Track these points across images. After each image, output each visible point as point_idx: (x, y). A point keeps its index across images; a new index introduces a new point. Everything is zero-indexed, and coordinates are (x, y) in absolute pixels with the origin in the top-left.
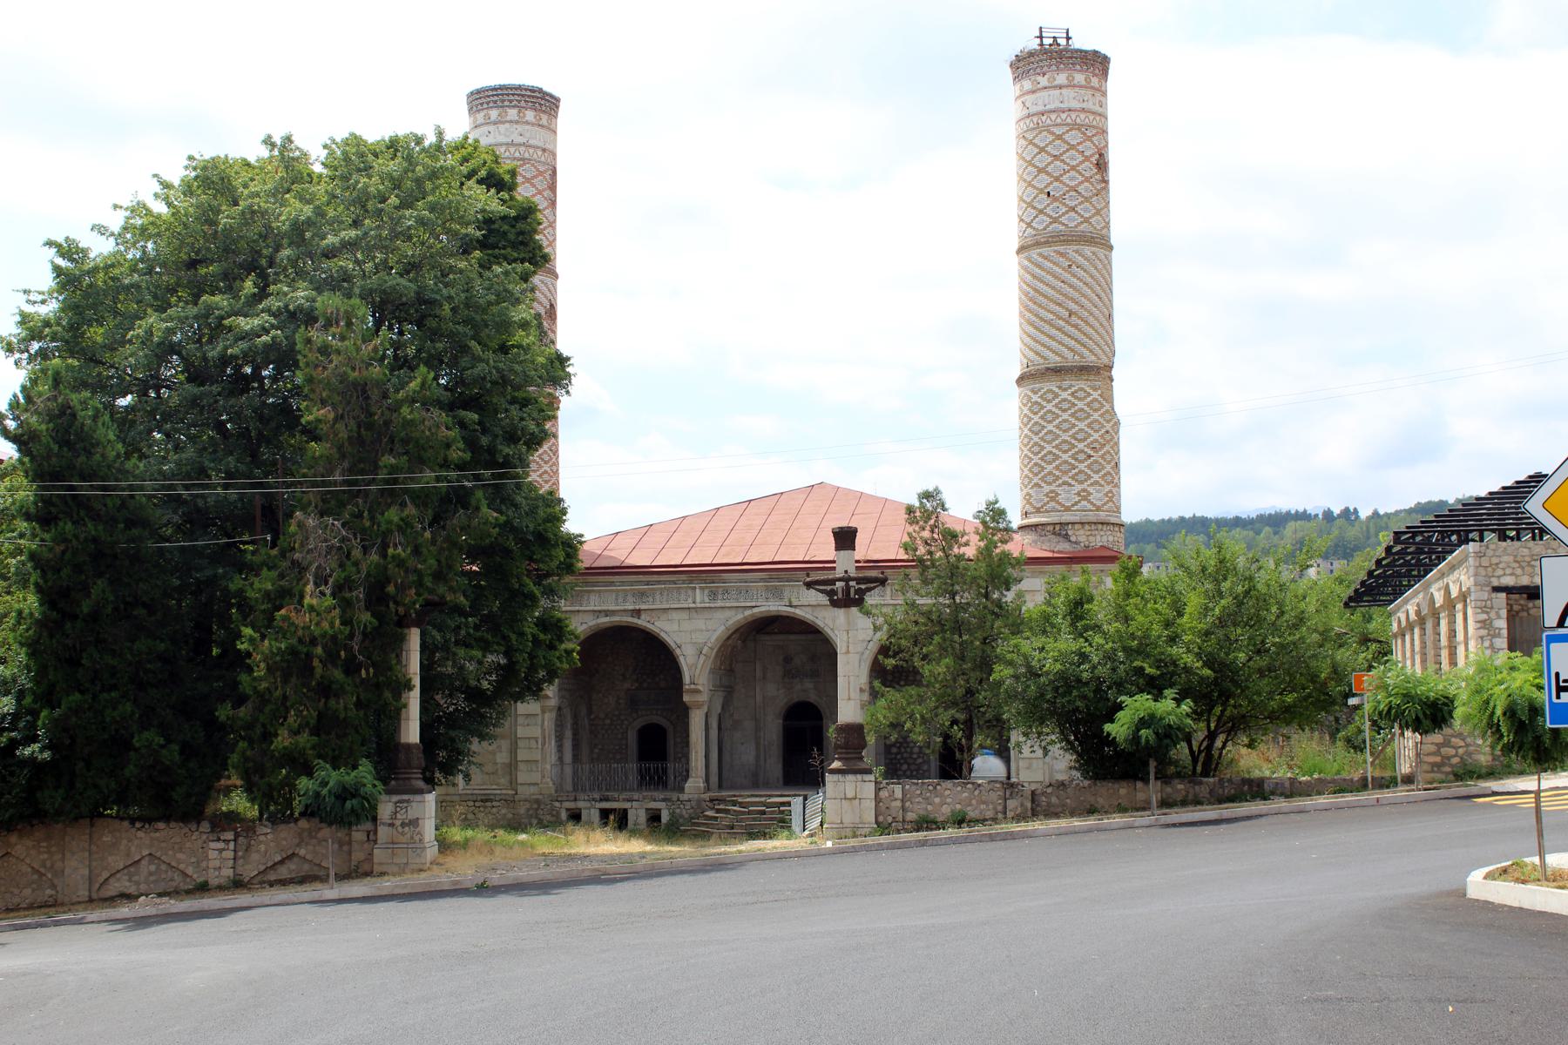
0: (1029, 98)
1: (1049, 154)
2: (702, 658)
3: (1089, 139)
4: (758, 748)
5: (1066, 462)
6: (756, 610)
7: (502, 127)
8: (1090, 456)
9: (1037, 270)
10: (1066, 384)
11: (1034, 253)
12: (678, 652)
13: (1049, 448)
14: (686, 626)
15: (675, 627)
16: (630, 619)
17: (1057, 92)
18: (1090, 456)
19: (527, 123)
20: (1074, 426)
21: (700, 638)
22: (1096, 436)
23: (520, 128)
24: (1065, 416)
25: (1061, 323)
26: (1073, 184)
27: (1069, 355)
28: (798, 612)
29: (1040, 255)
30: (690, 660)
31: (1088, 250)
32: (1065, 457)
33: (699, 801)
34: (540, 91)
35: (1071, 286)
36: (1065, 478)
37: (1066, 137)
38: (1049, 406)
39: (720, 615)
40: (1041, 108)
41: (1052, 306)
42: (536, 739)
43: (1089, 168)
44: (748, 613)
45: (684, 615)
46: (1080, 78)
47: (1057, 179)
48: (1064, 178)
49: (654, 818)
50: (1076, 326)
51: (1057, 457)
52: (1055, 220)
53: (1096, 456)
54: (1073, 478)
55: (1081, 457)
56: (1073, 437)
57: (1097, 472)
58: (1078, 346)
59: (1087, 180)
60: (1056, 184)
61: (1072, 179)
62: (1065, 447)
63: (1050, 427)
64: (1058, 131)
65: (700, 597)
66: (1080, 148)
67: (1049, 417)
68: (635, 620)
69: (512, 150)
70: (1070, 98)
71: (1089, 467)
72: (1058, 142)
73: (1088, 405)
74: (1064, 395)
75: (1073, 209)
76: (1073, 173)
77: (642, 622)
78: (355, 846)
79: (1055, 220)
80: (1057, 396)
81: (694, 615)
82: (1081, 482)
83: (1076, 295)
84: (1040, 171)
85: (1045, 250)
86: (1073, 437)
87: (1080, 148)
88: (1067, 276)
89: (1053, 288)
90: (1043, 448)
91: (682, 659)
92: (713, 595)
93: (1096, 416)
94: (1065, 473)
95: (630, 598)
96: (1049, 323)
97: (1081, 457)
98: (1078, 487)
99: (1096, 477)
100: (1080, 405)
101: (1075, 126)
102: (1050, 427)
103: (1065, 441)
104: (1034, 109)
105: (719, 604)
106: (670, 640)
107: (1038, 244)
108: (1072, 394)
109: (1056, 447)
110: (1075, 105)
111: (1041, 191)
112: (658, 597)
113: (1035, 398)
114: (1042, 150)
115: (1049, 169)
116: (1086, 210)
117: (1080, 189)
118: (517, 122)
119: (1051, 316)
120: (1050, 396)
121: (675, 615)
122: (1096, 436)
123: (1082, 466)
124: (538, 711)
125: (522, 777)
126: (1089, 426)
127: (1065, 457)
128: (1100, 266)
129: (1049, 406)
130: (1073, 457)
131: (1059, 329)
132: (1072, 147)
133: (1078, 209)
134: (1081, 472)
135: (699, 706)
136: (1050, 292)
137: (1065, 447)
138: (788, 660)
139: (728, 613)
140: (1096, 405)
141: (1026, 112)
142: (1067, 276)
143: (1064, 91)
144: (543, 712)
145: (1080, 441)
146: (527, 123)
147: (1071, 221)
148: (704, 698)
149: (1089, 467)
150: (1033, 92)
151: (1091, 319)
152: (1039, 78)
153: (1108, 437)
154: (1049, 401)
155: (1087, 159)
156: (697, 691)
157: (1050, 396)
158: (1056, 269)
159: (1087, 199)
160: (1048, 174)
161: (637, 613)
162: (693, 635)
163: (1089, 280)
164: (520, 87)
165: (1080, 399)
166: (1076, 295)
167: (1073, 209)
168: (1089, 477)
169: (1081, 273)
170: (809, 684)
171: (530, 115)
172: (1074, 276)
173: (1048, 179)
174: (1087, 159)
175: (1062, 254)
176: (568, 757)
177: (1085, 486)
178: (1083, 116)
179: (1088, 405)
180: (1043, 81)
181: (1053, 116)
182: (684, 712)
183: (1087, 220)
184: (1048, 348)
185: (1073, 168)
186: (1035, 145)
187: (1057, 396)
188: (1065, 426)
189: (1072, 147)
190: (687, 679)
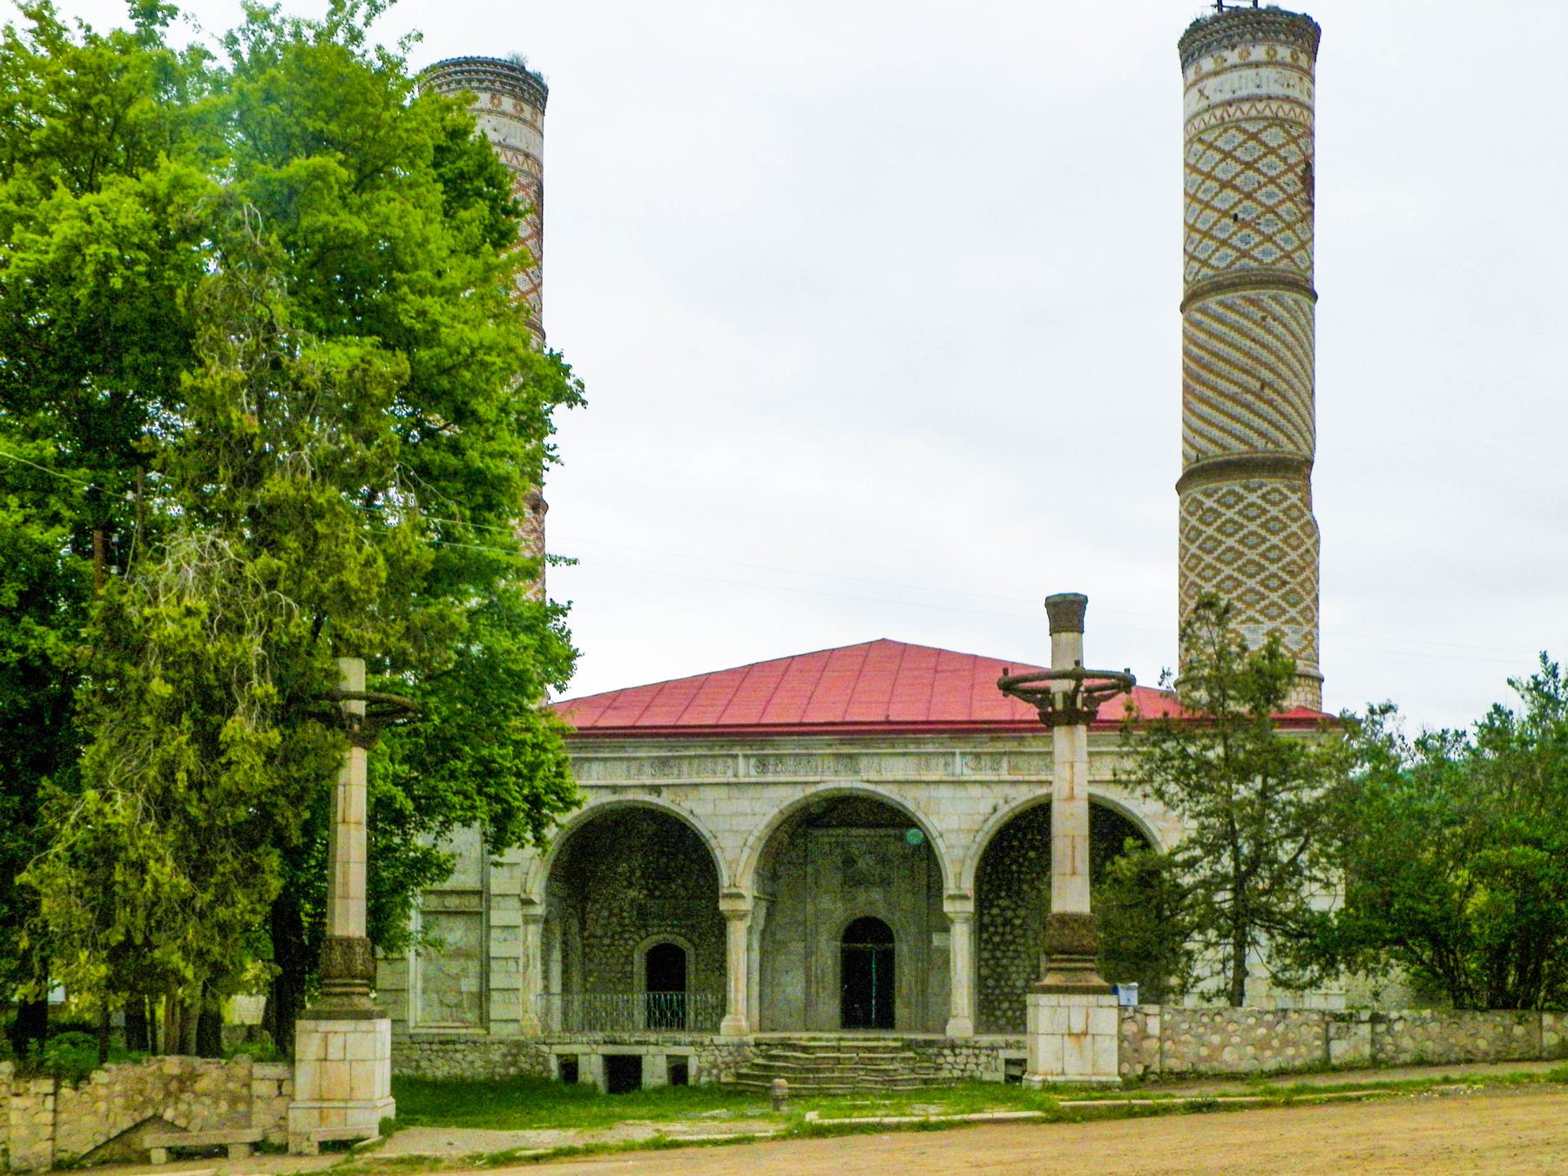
0: (1210, 84)
1: (1237, 160)
2: (747, 851)
3: (1295, 140)
5: (1252, 590)
6: (821, 787)
8: (1284, 583)
9: (1216, 326)
10: (1254, 481)
11: (1212, 303)
12: (713, 843)
13: (1227, 571)
14: (727, 807)
15: (710, 808)
17: (1253, 71)
18: (1284, 583)
20: (1264, 540)
21: (745, 824)
22: (1293, 555)
24: (1253, 526)
25: (1250, 398)
26: (1270, 202)
27: (1260, 443)
28: (880, 790)
29: (1221, 303)
31: (1289, 297)
32: (1251, 583)
35: (1264, 346)
36: (1251, 613)
37: (1264, 136)
38: (1230, 514)
39: (769, 792)
40: (1228, 96)
41: (1237, 374)
43: (1291, 181)
44: (810, 790)
46: (1284, 53)
47: (1249, 196)
48: (1259, 195)
49: (678, 1072)
50: (1270, 403)
51: (1239, 583)
52: (1245, 254)
53: (1293, 583)
54: (1261, 612)
55: (1274, 583)
56: (1263, 555)
57: (1294, 605)
58: (1271, 430)
59: (1290, 198)
60: (1247, 203)
61: (1270, 195)
62: (1252, 569)
63: (1230, 542)
64: (1252, 128)
65: (745, 769)
66: (1282, 152)
67: (1229, 528)
70: (1271, 81)
71: (1283, 597)
72: (1251, 143)
73: (1285, 512)
74: (1252, 498)
75: (1269, 238)
76: (1271, 188)
77: (664, 801)
78: (259, 1106)
79: (1245, 254)
80: (1240, 498)
81: (735, 792)
82: (1272, 618)
83: (1272, 359)
84: (1224, 185)
85: (1229, 297)
86: (1263, 555)
87: (1282, 152)
88: (1258, 332)
89: (1239, 349)
90: (1219, 571)
91: (718, 852)
92: (763, 763)
93: (1294, 527)
94: (1250, 605)
95: (647, 769)
96: (1234, 399)
97: (1274, 583)
98: (1269, 625)
99: (1293, 612)
100: (1274, 511)
101: (1276, 121)
102: (1230, 542)
103: (1250, 562)
104: (1217, 98)
105: (770, 778)
106: (703, 826)
107: (1218, 287)
108: (1263, 497)
109: (1239, 569)
110: (1276, 90)
111: (1225, 214)
113: (1209, 503)
114: (1227, 155)
115: (1238, 182)
116: (1287, 240)
117: (1280, 210)
119: (1235, 389)
120: (1231, 499)
121: (708, 793)
122: (1293, 555)
123: (1274, 597)
124: (520, 921)
125: (497, 1010)
126: (1285, 540)
127: (1251, 583)
128: (1303, 321)
129: (1230, 514)
130: (1262, 583)
131: (1247, 406)
132: (1272, 151)
133: (1277, 238)
134: (1273, 604)
135: (741, 916)
136: (1235, 355)
137: (1252, 569)
140: (1295, 513)
141: (1205, 103)
142: (1258, 332)
143: (1263, 71)
144: (527, 920)
145: (1272, 561)
147: (1267, 255)
148: (746, 905)
149: (1283, 597)
150: (1216, 73)
151: (1291, 394)
152: (1227, 54)
153: (1308, 558)
154: (1229, 507)
155: (1291, 168)
156: (740, 896)
157: (1231, 499)
158: (1243, 321)
159: (1289, 226)
160: (1235, 188)
161: (656, 789)
162: (736, 814)
163: (1289, 338)
165: (1274, 504)
166: (1272, 359)
167: (1269, 238)
168: (1284, 612)
169: (1280, 329)
172: (1270, 332)
173: (1234, 196)
174: (1291, 168)
175: (1252, 302)
177: (1277, 623)
178: (1287, 107)
179: (1285, 512)
180: (1233, 57)
181: (1246, 107)
182: (719, 926)
183: (1288, 256)
184: (1230, 433)
185: (1272, 180)
186: (1218, 149)
187: (1240, 498)
188: (1252, 540)
189: (1272, 151)
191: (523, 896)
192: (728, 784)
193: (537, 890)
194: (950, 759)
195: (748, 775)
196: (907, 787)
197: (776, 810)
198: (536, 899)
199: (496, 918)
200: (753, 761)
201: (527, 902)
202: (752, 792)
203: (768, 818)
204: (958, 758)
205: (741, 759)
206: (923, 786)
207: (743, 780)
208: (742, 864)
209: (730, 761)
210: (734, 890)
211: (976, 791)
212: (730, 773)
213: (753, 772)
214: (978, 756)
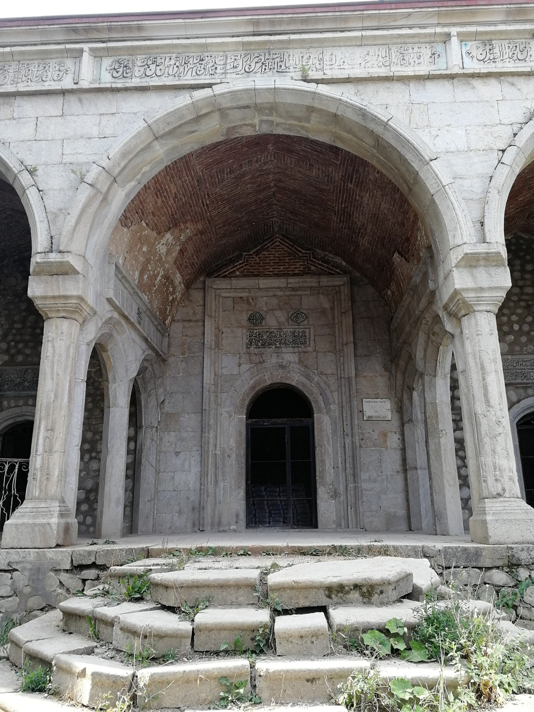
2: (85, 192)
4: (203, 463)
12: (25, 179)
15: (28, 131)
21: (83, 153)
33: (38, 573)
39: (134, 104)
92: (123, 68)
105: (135, 82)
121: (29, 108)
138: (255, 319)
156: (64, 271)
170: (289, 356)
190: (39, 241)
192: (63, 92)
194: (439, 48)
196: (371, 88)
200: (107, 62)
202: (104, 104)
204: (455, 40)
205: (86, 56)
206: (398, 87)
208: (75, 212)
209: (69, 63)
210: (54, 257)
211: (490, 90)
214: (487, 41)
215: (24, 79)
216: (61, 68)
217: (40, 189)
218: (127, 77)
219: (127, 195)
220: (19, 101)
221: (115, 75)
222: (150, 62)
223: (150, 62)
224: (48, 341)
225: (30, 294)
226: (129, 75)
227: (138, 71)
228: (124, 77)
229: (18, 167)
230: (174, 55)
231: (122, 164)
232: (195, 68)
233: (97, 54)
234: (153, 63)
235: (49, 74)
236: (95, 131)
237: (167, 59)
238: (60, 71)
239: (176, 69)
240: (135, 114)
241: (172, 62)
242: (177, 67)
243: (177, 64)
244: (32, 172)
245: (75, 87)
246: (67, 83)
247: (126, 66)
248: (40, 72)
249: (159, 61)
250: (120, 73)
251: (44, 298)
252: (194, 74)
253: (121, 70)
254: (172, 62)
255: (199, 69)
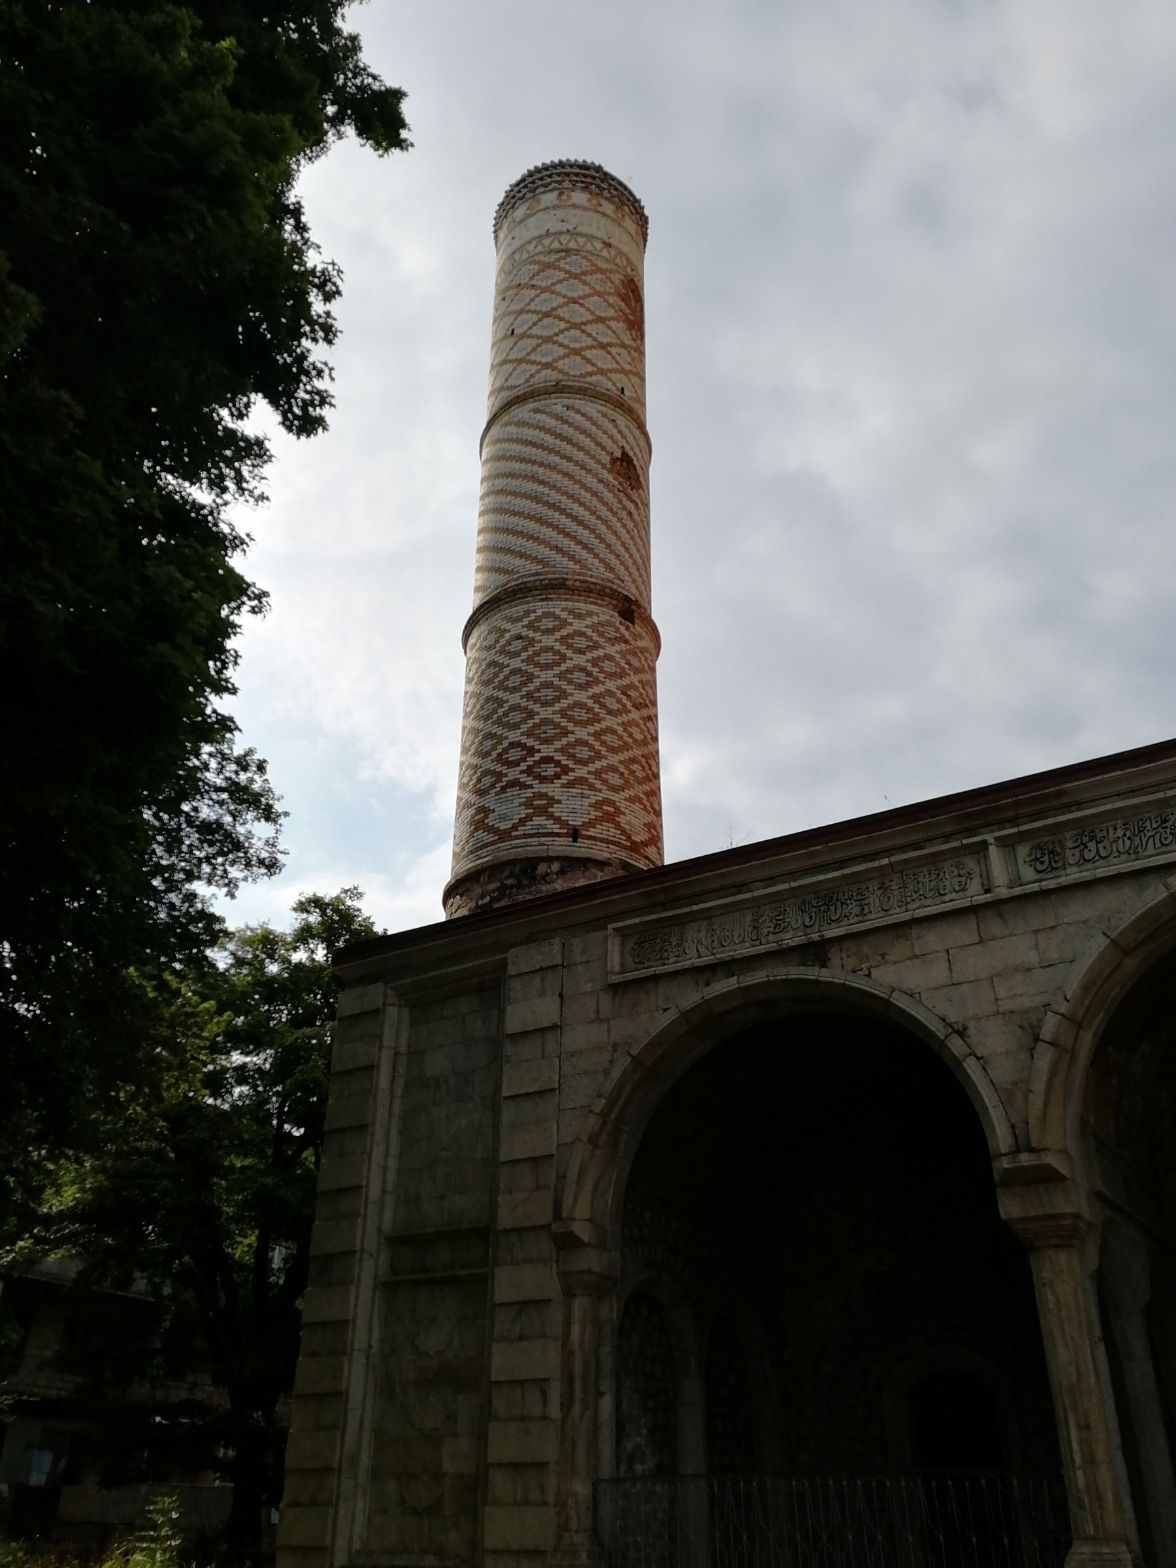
7: (531, 222)
12: (956, 1046)
14: (973, 963)
15: (938, 973)
16: (796, 972)
19: (574, 206)
21: (1025, 994)
23: (561, 214)
30: (1004, 1070)
34: (599, 169)
39: (1079, 909)
42: (541, 1384)
45: (962, 933)
68: (813, 973)
69: (547, 242)
77: (836, 972)
81: (995, 927)
91: (971, 1067)
92: (1048, 855)
95: (795, 919)
105: (1072, 875)
112: (873, 899)
118: (555, 207)
121: (932, 940)
135: (1067, 1234)
139: (1108, 899)
144: (570, 1286)
146: (574, 206)
148: (1075, 1201)
156: (1045, 1177)
161: (816, 952)
164: (561, 164)
171: (579, 197)
176: (693, 1458)
190: (1001, 1137)
191: (556, 1227)
192: (974, 910)
193: (587, 1207)
195: (1016, 881)
197: (1099, 944)
198: (583, 1231)
199: (509, 1283)
200: (1023, 851)
201: (567, 1242)
203: (1084, 965)
205: (994, 852)
207: (1003, 892)
209: (970, 863)
210: (1025, 1159)
212: (975, 886)
213: (1028, 873)
215: (915, 896)
216: (962, 872)
217: (979, 1055)
218: (1057, 868)
219: (1094, 1035)
220: (915, 931)
221: (1040, 867)
222: (1085, 840)
223: (1085, 840)
224: (1044, 1285)
225: (1003, 1215)
226: (1059, 864)
227: (1071, 856)
228: (1053, 869)
229: (942, 1029)
230: (1119, 822)
231: (1087, 1003)
232: (1158, 836)
233: (1006, 844)
234: (1091, 840)
235: (947, 883)
236: (1033, 958)
237: (1111, 830)
238: (960, 876)
239: (1128, 843)
240: (1085, 922)
241: (1120, 833)
242: (1129, 838)
243: (1128, 833)
244: (962, 1033)
245: (988, 897)
246: (975, 894)
247: (1051, 852)
248: (934, 883)
249: (1099, 835)
250: (1046, 864)
251: (1026, 1219)
252: (1158, 844)
253: (1046, 858)
254: (1120, 833)
255: (1164, 835)
